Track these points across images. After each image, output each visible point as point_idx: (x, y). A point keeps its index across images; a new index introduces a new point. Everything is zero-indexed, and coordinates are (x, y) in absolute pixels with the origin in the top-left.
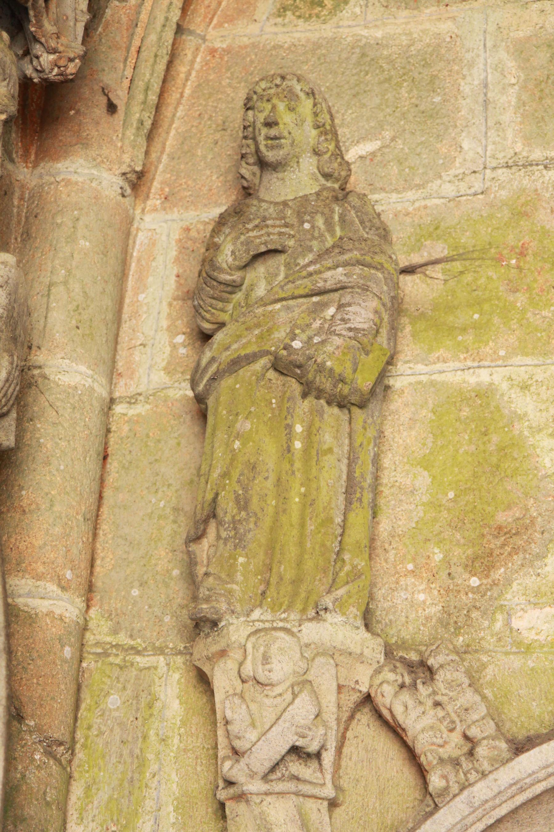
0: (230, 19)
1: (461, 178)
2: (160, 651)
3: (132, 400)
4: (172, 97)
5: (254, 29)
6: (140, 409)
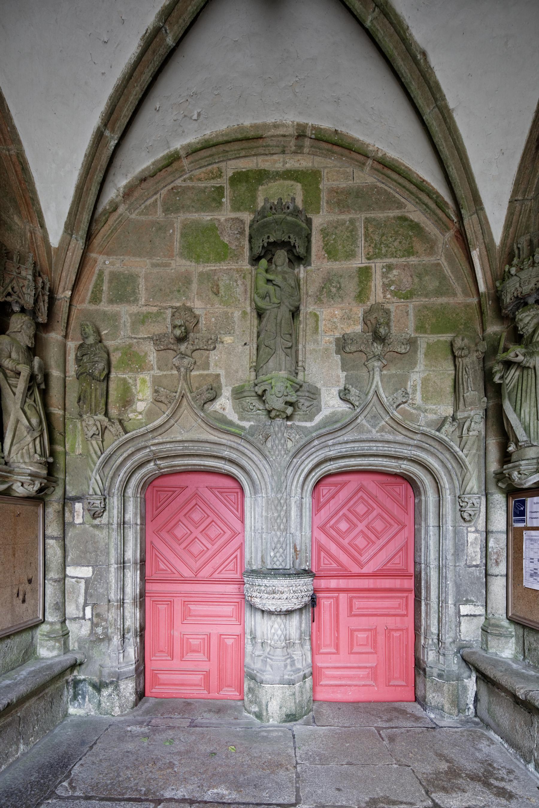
4: (71, 319)
5: (85, 305)
6: (71, 379)
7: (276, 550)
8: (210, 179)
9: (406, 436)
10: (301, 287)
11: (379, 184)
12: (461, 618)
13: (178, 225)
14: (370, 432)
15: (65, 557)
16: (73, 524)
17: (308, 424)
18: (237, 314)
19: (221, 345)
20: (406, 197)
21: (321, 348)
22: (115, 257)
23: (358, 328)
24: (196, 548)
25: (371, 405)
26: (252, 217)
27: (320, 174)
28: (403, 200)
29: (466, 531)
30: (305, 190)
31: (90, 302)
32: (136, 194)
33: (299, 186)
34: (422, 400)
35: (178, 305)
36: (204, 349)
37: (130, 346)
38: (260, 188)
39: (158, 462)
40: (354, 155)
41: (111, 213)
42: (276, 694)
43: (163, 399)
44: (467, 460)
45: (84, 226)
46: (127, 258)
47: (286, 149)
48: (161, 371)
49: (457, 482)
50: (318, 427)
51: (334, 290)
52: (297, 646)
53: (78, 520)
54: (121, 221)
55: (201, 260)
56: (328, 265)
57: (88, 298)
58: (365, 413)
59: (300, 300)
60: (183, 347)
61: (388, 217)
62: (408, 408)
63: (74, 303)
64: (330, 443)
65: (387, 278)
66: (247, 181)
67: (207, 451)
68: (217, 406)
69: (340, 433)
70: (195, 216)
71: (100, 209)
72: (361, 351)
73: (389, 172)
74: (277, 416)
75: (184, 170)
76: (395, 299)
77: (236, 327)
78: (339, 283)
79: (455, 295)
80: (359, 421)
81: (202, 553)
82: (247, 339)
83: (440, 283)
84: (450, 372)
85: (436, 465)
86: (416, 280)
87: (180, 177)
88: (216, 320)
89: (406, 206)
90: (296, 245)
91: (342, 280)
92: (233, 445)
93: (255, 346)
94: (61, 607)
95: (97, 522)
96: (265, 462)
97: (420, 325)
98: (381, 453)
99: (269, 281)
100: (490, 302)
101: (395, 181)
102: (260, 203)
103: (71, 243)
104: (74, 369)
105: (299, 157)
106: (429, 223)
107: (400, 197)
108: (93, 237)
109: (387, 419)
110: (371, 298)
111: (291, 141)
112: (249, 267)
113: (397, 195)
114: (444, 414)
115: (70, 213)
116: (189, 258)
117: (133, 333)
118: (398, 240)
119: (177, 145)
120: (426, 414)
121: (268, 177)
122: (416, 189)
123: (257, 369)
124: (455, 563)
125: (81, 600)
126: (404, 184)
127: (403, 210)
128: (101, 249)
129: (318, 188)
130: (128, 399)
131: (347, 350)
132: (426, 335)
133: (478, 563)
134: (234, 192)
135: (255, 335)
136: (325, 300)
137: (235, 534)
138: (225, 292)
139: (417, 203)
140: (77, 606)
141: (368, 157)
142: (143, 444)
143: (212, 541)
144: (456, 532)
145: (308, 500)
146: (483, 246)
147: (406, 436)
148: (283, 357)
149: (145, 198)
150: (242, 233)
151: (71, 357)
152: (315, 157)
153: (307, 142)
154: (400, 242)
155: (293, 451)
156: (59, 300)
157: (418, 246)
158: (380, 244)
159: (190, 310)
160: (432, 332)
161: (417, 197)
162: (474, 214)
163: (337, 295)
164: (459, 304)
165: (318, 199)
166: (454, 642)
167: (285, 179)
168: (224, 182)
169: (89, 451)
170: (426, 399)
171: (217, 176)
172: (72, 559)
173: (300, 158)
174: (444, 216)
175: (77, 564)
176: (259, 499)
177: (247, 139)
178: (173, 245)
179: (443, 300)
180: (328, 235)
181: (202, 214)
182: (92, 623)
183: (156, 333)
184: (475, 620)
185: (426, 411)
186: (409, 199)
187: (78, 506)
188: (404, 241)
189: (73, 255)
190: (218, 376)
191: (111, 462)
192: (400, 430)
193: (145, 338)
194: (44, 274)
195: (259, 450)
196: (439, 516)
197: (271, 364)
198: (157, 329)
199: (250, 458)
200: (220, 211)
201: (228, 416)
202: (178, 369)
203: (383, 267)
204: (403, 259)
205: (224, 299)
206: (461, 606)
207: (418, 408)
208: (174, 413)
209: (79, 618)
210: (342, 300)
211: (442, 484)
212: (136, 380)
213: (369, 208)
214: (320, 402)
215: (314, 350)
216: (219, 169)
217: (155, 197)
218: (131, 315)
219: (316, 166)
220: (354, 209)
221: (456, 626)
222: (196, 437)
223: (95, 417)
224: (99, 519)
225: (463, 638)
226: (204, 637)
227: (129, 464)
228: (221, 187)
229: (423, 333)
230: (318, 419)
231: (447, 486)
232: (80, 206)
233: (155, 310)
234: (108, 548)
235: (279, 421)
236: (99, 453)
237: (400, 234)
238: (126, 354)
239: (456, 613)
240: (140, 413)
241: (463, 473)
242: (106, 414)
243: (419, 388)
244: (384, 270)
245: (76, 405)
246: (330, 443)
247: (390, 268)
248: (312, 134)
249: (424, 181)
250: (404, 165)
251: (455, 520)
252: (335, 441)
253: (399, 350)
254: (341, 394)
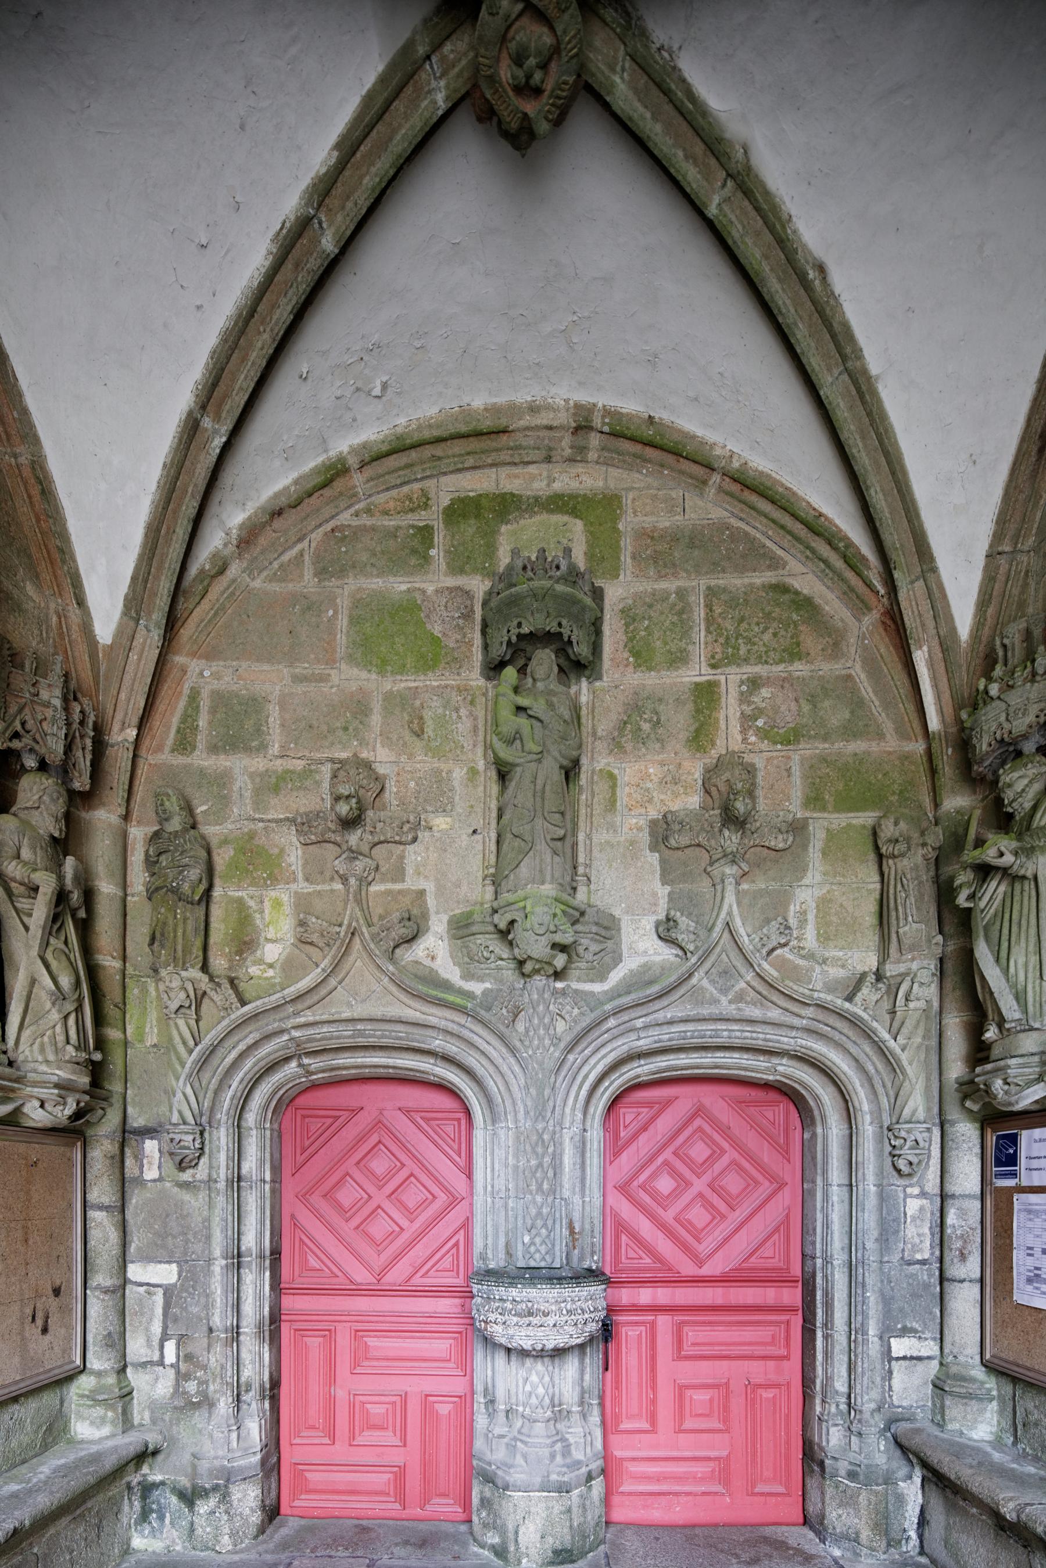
0: (155, 752)
1: (233, 822)
2: (149, 977)
3: (133, 895)
4: (137, 783)
5: (163, 757)
6: (136, 899)
7: (534, 1232)
8: (406, 513)
9: (787, 1010)
10: (583, 720)
11: (734, 522)
12: (893, 1363)
13: (344, 602)
14: (717, 1001)
15: (124, 1245)
16: (140, 1181)
17: (597, 988)
18: (459, 774)
19: (427, 834)
20: (786, 545)
21: (622, 839)
22: (222, 663)
23: (694, 801)
24: (380, 1227)
25: (718, 949)
26: (488, 584)
27: (620, 502)
28: (780, 552)
29: (902, 1195)
30: (591, 533)
31: (173, 751)
32: (263, 541)
33: (578, 525)
34: (818, 940)
35: (344, 755)
36: (395, 842)
37: (252, 835)
38: (504, 528)
39: (306, 1061)
40: (686, 465)
41: (213, 577)
42: (533, 1510)
43: (315, 938)
44: (904, 1057)
45: (162, 602)
46: (244, 664)
47: (553, 453)
48: (312, 883)
49: (885, 1100)
50: (615, 994)
51: (646, 727)
52: (576, 1418)
53: (151, 1173)
54: (233, 593)
55: (389, 668)
56: (636, 679)
57: (170, 741)
58: (707, 965)
59: (580, 746)
60: (354, 838)
61: (751, 585)
62: (790, 956)
63: (143, 752)
64: (639, 1023)
65: (749, 703)
66: (477, 516)
67: (400, 1038)
68: (419, 951)
69: (658, 1005)
70: (376, 583)
71: (193, 570)
72: (699, 845)
73: (753, 498)
74: (537, 971)
75: (355, 495)
76: (765, 745)
77: (457, 798)
78: (657, 713)
79: (881, 736)
80: (694, 980)
81: (391, 1236)
82: (478, 823)
83: (852, 712)
84: (872, 886)
85: (845, 1067)
86: (806, 708)
87: (349, 507)
88: (417, 784)
89: (785, 564)
90: (574, 639)
91: (661, 708)
92: (451, 1026)
93: (493, 836)
94: (117, 1342)
95: (186, 1176)
96: (512, 1060)
97: (813, 795)
98: (738, 1042)
99: (520, 709)
100: (950, 751)
101: (766, 516)
102: (504, 559)
103: (137, 636)
104: (142, 881)
105: (579, 468)
106: (830, 596)
107: (774, 548)
108: (180, 623)
109: (750, 976)
110: (718, 742)
111: (563, 437)
112: (482, 682)
113: (769, 543)
114: (860, 968)
115: (134, 579)
116: (366, 665)
117: (256, 809)
118: (771, 631)
119: (342, 445)
120: (826, 968)
121: (519, 508)
122: (806, 530)
123: (497, 881)
124: (882, 1256)
125: (157, 1328)
126: (782, 522)
127: (781, 572)
128: (195, 648)
129: (616, 530)
130: (247, 939)
131: (673, 843)
132: (826, 815)
133: (926, 1256)
134: (453, 536)
135: (494, 814)
136: (629, 747)
137: (454, 1201)
138: (434, 730)
139: (807, 557)
140: (149, 1341)
141: (713, 470)
142: (276, 1025)
143: (411, 1214)
144: (883, 1197)
145: (595, 1134)
146: (935, 643)
147: (787, 1010)
148: (548, 856)
149: (280, 549)
150: (468, 616)
151: (137, 858)
152: (610, 469)
153: (594, 440)
154: (775, 635)
155: (568, 1038)
156: (112, 746)
157: (810, 641)
158: (737, 639)
159: (368, 765)
160: (837, 810)
161: (808, 547)
162: (917, 579)
163: (652, 736)
164: (890, 753)
165: (616, 549)
166: (879, 1409)
167: (551, 511)
168: (433, 517)
169: (171, 1039)
170: (824, 938)
171: (419, 506)
172: (139, 1249)
173: (580, 470)
174: (860, 583)
175: (148, 1258)
176: (502, 1133)
177: (478, 434)
178: (335, 639)
179: (858, 746)
180: (634, 620)
181: (392, 579)
182: (178, 1372)
183: (302, 810)
184: (920, 1366)
185: (825, 961)
186: (792, 551)
187: (151, 1146)
188: (783, 633)
189: (139, 660)
190: (422, 893)
191: (215, 1061)
192: (774, 998)
193: (281, 820)
194: (84, 696)
195: (502, 1038)
196: (851, 1165)
197: (524, 870)
198: (304, 802)
199: (483, 1053)
200: (427, 573)
201: (440, 971)
202: (344, 879)
203: (742, 682)
204: (781, 667)
205: (433, 744)
206: (892, 1340)
207: (810, 956)
208: (336, 966)
209: (151, 1363)
210: (663, 747)
211: (857, 1104)
212: (262, 902)
213: (716, 567)
214: (618, 944)
215: (608, 842)
216: (424, 493)
217: (299, 547)
218: (252, 776)
219: (612, 486)
220: (686, 571)
221: (883, 1379)
222: (378, 1012)
223: (184, 974)
224: (190, 1172)
225: (896, 1403)
226: (394, 1399)
227: (249, 1063)
228: (427, 526)
229: (820, 811)
230: (616, 976)
231: (866, 1107)
232: (155, 564)
233: (299, 765)
234: (209, 1228)
235: (539, 981)
236: (191, 1043)
237: (774, 619)
238: (242, 851)
239: (883, 1354)
240: (271, 966)
241: (897, 1083)
242: (205, 968)
243: (811, 917)
244: (744, 688)
245: (147, 950)
246: (639, 1023)
247: (754, 683)
248: (604, 424)
249: (821, 515)
250: (782, 485)
251: (880, 1173)
252: (648, 1019)
253: (773, 843)
254: (661, 929)
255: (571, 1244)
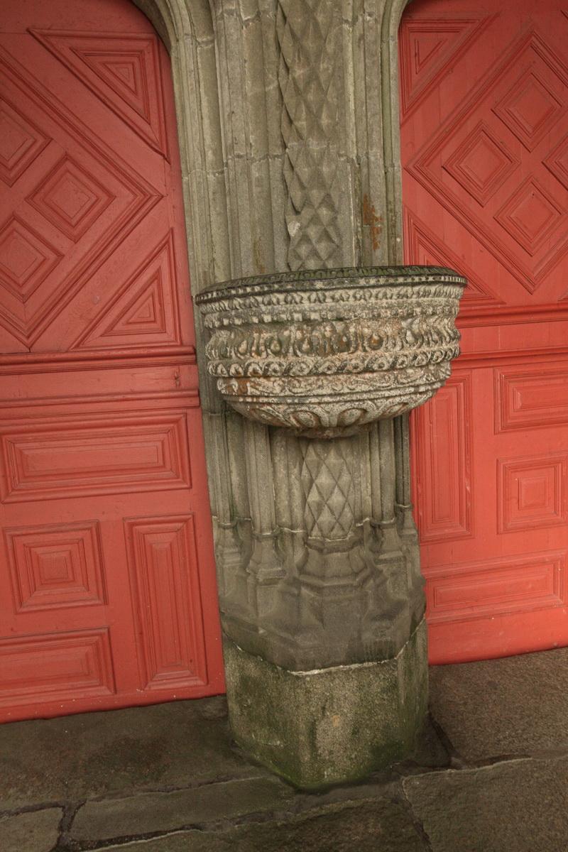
7: (306, 214)
42: (337, 693)
226: (79, 535)
255: (367, 241)
